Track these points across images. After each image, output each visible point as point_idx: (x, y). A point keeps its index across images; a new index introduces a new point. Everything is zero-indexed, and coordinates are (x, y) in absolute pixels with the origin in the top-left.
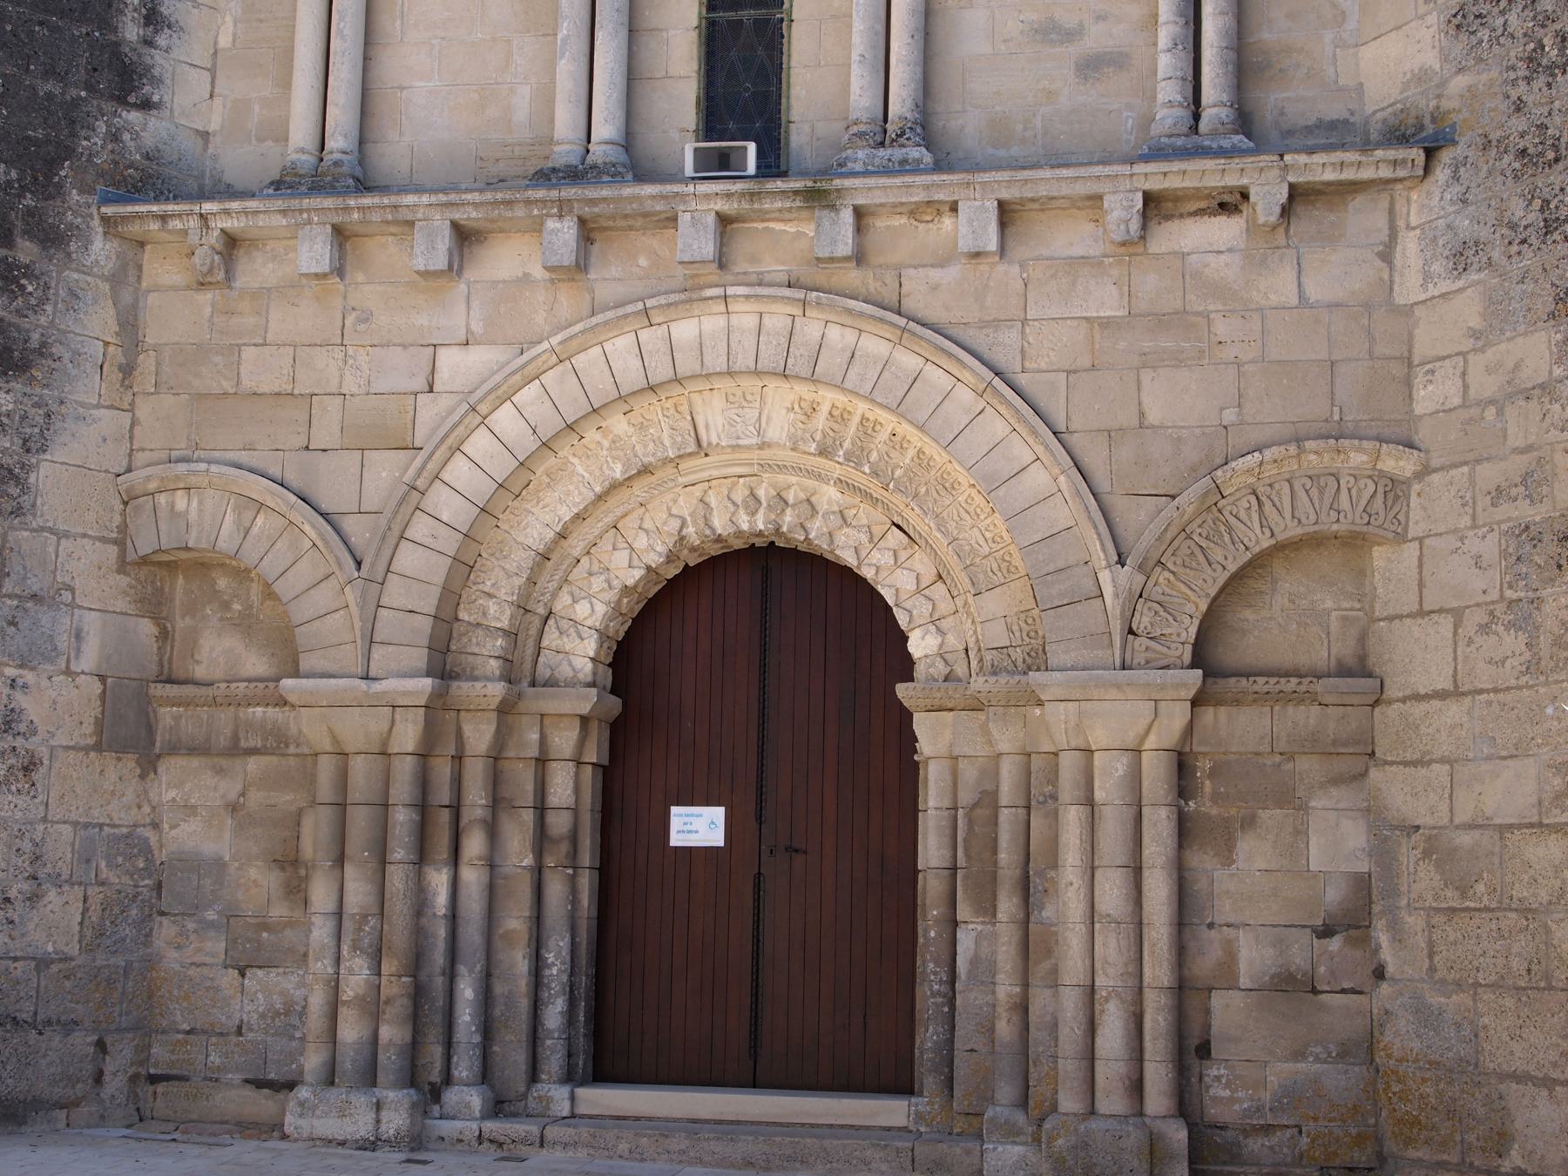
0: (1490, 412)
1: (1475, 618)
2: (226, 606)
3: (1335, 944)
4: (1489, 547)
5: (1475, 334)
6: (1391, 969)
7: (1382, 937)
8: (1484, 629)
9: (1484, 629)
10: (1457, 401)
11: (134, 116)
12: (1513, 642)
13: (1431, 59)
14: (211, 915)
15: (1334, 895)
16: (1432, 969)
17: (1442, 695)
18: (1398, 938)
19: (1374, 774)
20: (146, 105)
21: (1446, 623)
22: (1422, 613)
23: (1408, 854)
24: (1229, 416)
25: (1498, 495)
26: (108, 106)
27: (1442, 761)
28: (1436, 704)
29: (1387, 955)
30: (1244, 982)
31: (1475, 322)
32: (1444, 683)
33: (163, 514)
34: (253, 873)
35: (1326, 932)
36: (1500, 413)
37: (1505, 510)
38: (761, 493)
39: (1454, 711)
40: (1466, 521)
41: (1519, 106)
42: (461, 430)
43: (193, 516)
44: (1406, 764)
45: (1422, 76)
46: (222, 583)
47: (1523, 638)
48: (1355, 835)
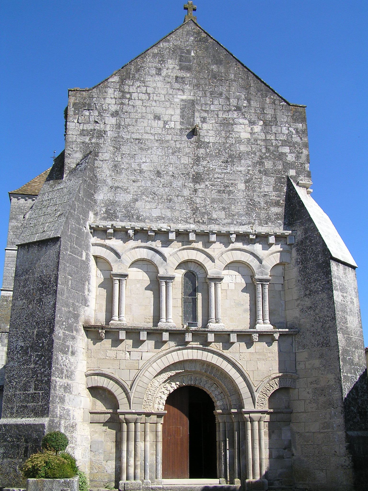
0: (310, 371)
1: (308, 401)
2: (101, 396)
3: (286, 450)
4: (310, 391)
5: (307, 358)
6: (295, 454)
7: (293, 449)
8: (310, 403)
9: (310, 403)
10: (303, 368)
11: (86, 308)
12: (314, 405)
13: (298, 315)
14: (100, 451)
15: (286, 443)
16: (302, 454)
17: (303, 412)
18: (296, 450)
19: (291, 424)
20: (88, 306)
21: (303, 402)
22: (299, 400)
23: (297, 437)
24: (271, 369)
25: (311, 383)
26: (84, 307)
27: (303, 422)
28: (302, 414)
29: (294, 452)
30: (273, 457)
31: (307, 357)
32: (303, 410)
33: (93, 380)
34: (108, 444)
35: (285, 449)
36: (311, 371)
37: (313, 385)
38: (192, 377)
39: (305, 415)
40: (306, 386)
41: (313, 326)
42: (147, 367)
43: (99, 380)
44: (297, 423)
45: (296, 318)
46: (101, 391)
47: (316, 404)
48: (289, 434)
